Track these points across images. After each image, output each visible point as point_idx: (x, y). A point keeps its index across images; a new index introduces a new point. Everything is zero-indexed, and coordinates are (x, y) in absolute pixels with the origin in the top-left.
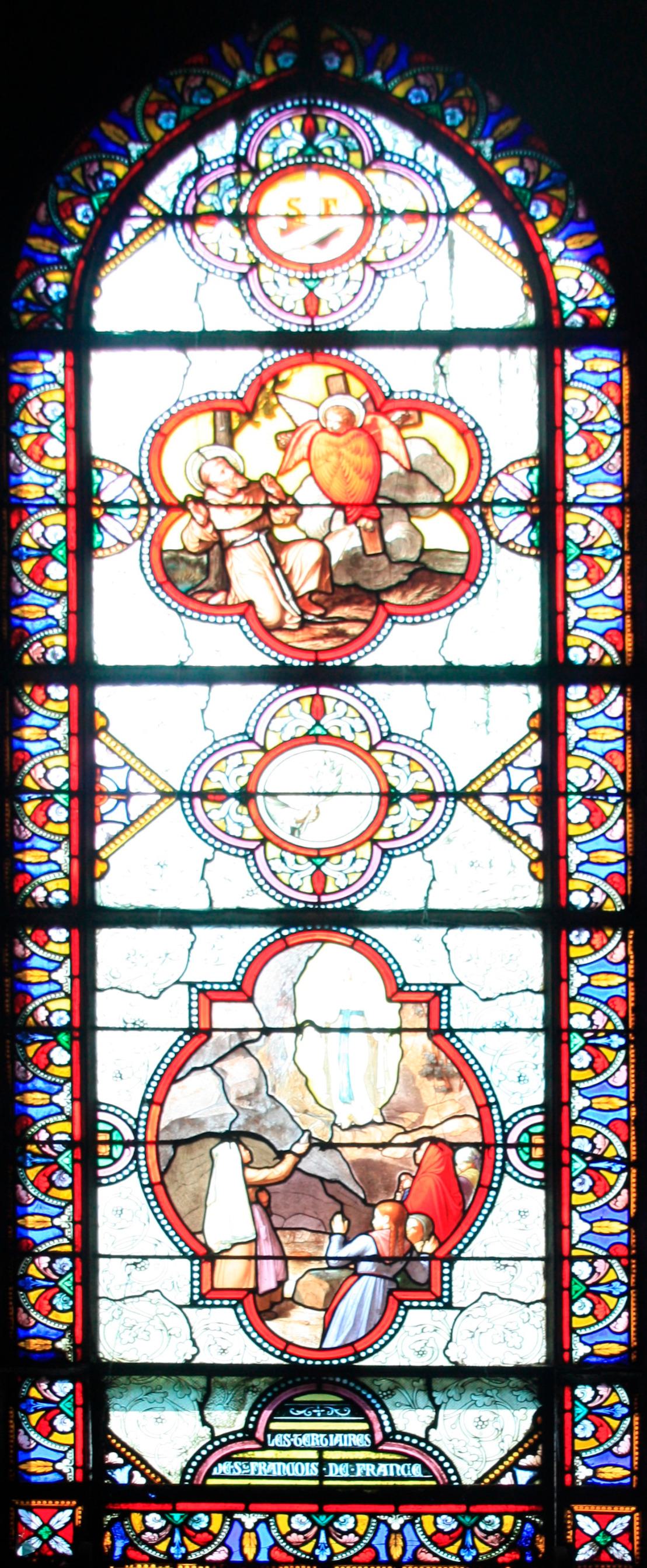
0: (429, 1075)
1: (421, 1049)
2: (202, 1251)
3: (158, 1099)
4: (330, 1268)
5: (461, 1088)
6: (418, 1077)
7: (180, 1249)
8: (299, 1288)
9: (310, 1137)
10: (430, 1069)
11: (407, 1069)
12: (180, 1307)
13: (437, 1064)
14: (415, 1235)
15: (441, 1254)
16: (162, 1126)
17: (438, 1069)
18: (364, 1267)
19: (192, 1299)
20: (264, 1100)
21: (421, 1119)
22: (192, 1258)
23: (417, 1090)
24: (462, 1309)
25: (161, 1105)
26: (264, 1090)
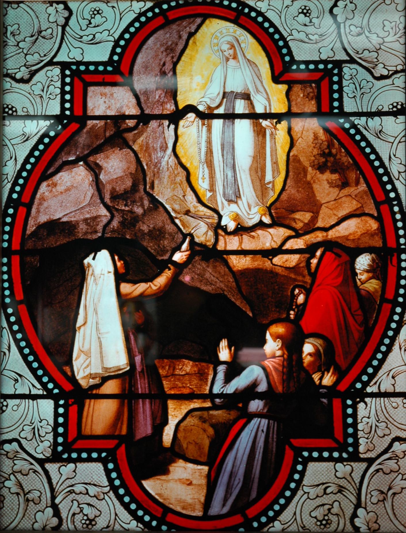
0: (321, 168)
1: (312, 136)
2: (68, 387)
3: (26, 199)
4: (215, 407)
5: (357, 183)
6: (310, 169)
7: (44, 386)
8: (180, 435)
9: (192, 243)
10: (323, 160)
11: (297, 160)
12: (41, 462)
13: (330, 154)
14: (310, 364)
15: (342, 387)
16: (28, 232)
17: (332, 159)
18: (255, 405)
20: (141, 199)
21: (314, 219)
22: (56, 398)
23: (309, 186)
24: (370, 461)
25: (29, 206)
26: (141, 187)
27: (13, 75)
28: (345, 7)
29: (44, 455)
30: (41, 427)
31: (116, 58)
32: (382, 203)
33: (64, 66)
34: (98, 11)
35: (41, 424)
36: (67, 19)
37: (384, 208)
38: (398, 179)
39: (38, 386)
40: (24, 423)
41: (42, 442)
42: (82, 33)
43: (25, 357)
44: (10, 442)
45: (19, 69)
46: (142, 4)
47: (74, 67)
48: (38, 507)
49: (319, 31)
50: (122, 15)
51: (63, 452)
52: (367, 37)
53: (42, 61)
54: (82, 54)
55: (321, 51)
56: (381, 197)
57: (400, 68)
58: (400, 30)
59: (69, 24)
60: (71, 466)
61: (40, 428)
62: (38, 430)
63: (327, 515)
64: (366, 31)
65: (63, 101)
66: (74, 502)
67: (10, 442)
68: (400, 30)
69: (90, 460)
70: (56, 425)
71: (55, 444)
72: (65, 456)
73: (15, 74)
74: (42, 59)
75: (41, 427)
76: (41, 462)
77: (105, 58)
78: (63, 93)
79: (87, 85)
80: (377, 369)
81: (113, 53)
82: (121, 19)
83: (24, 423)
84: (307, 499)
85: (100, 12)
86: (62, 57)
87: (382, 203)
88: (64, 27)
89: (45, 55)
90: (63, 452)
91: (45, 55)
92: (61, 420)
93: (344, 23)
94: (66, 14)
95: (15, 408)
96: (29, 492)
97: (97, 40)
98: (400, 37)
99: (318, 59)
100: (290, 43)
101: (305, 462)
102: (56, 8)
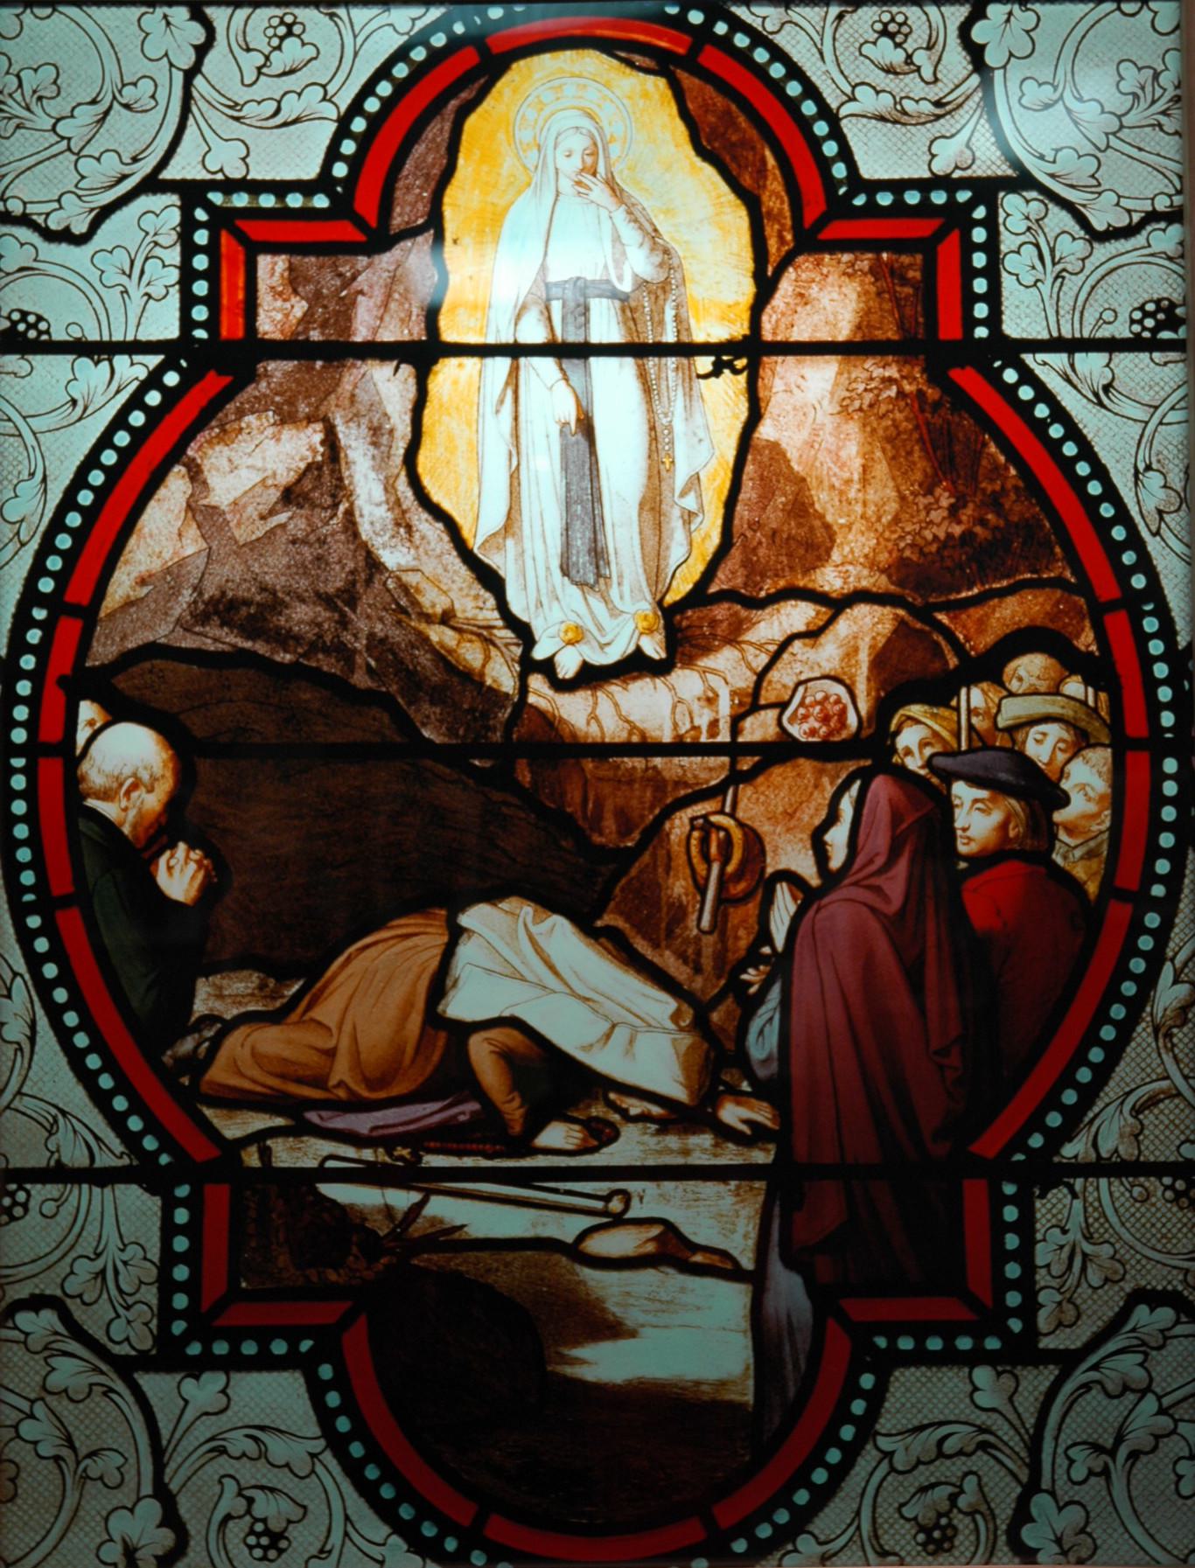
3: (78, 593)
7: (131, 1141)
12: (126, 1367)
19: (163, 1337)
27: (40, 220)
28: (1008, 20)
29: (133, 1348)
30: (125, 1263)
31: (340, 170)
32: (1112, 606)
33: (191, 193)
34: (290, 27)
35: (125, 1257)
36: (202, 51)
37: (1117, 622)
38: (1157, 533)
39: (116, 1144)
40: (79, 1250)
41: (128, 1308)
42: (240, 95)
43: (76, 1059)
44: (36, 1303)
45: (59, 201)
46: (416, 11)
47: (216, 198)
48: (121, 1497)
49: (935, 92)
50: (359, 40)
51: (187, 1337)
52: (1069, 111)
53: (124, 177)
54: (243, 159)
55: (934, 151)
56: (1107, 590)
57: (1162, 204)
58: (1165, 90)
59: (204, 69)
61: (120, 1266)
62: (116, 1272)
63: (947, 1514)
64: (1068, 96)
65: (188, 300)
66: (226, 1481)
68: (1165, 90)
70: (169, 1258)
71: (166, 1313)
72: (195, 1349)
73: (48, 215)
74: (127, 170)
75: (125, 1263)
76: (126, 1367)
77: (310, 171)
78: (188, 274)
79: (253, 250)
80: (1089, 1094)
81: (333, 154)
82: (356, 54)
83: (79, 1250)
84: (888, 1474)
85: (297, 29)
86: (183, 168)
87: (1112, 606)
88: (190, 75)
89: (135, 160)
90: (187, 1337)
91: (135, 160)
92: (181, 1244)
93: (1004, 67)
94: (197, 33)
95: (49, 1208)
96: (93, 1454)
98: (1164, 113)
99: (927, 175)
100: (846, 125)
102: (165, 17)
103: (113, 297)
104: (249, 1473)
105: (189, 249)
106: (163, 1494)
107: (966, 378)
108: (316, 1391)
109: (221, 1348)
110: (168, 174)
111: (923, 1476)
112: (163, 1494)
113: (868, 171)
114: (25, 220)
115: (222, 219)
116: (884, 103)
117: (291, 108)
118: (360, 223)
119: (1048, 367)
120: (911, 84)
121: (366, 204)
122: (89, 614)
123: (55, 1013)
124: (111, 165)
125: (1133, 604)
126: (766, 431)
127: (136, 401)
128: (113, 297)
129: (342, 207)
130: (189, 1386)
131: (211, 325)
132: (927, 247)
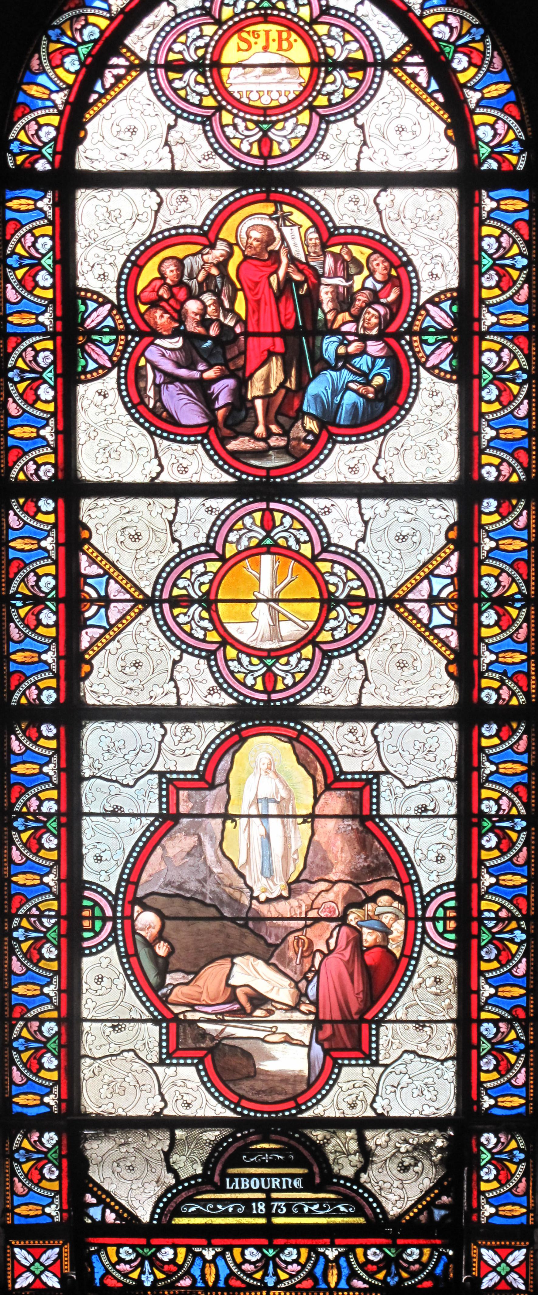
3: (134, 879)
12: (151, 1065)
19: (161, 1059)
32: (406, 884)
33: (162, 774)
36: (163, 736)
42: (174, 748)
43: (136, 993)
44: (128, 1051)
46: (222, 724)
56: (405, 880)
60: (173, 1069)
65: (161, 803)
67: (128, 1051)
69: (185, 1064)
76: (151, 1065)
77: (193, 768)
78: (161, 797)
79: (178, 789)
80: (395, 1004)
87: (406, 884)
97: (187, 753)
101: (341, 1066)
103: (141, 802)
104: (183, 1090)
105: (161, 789)
106: (161, 1094)
107: (369, 824)
108: (198, 1071)
109: (174, 1061)
110: (155, 769)
111: (349, 1092)
112: (161, 1094)
113: (345, 769)
114: (116, 781)
115: (170, 781)
116: (350, 751)
117: (188, 751)
118: (207, 782)
119: (392, 822)
120: (357, 746)
121: (208, 777)
122: (137, 884)
123: (131, 982)
124: (140, 767)
125: (411, 883)
126: (316, 838)
127: (147, 829)
128: (141, 802)
129: (202, 778)
130: (167, 1070)
131: (167, 809)
132: (361, 790)
